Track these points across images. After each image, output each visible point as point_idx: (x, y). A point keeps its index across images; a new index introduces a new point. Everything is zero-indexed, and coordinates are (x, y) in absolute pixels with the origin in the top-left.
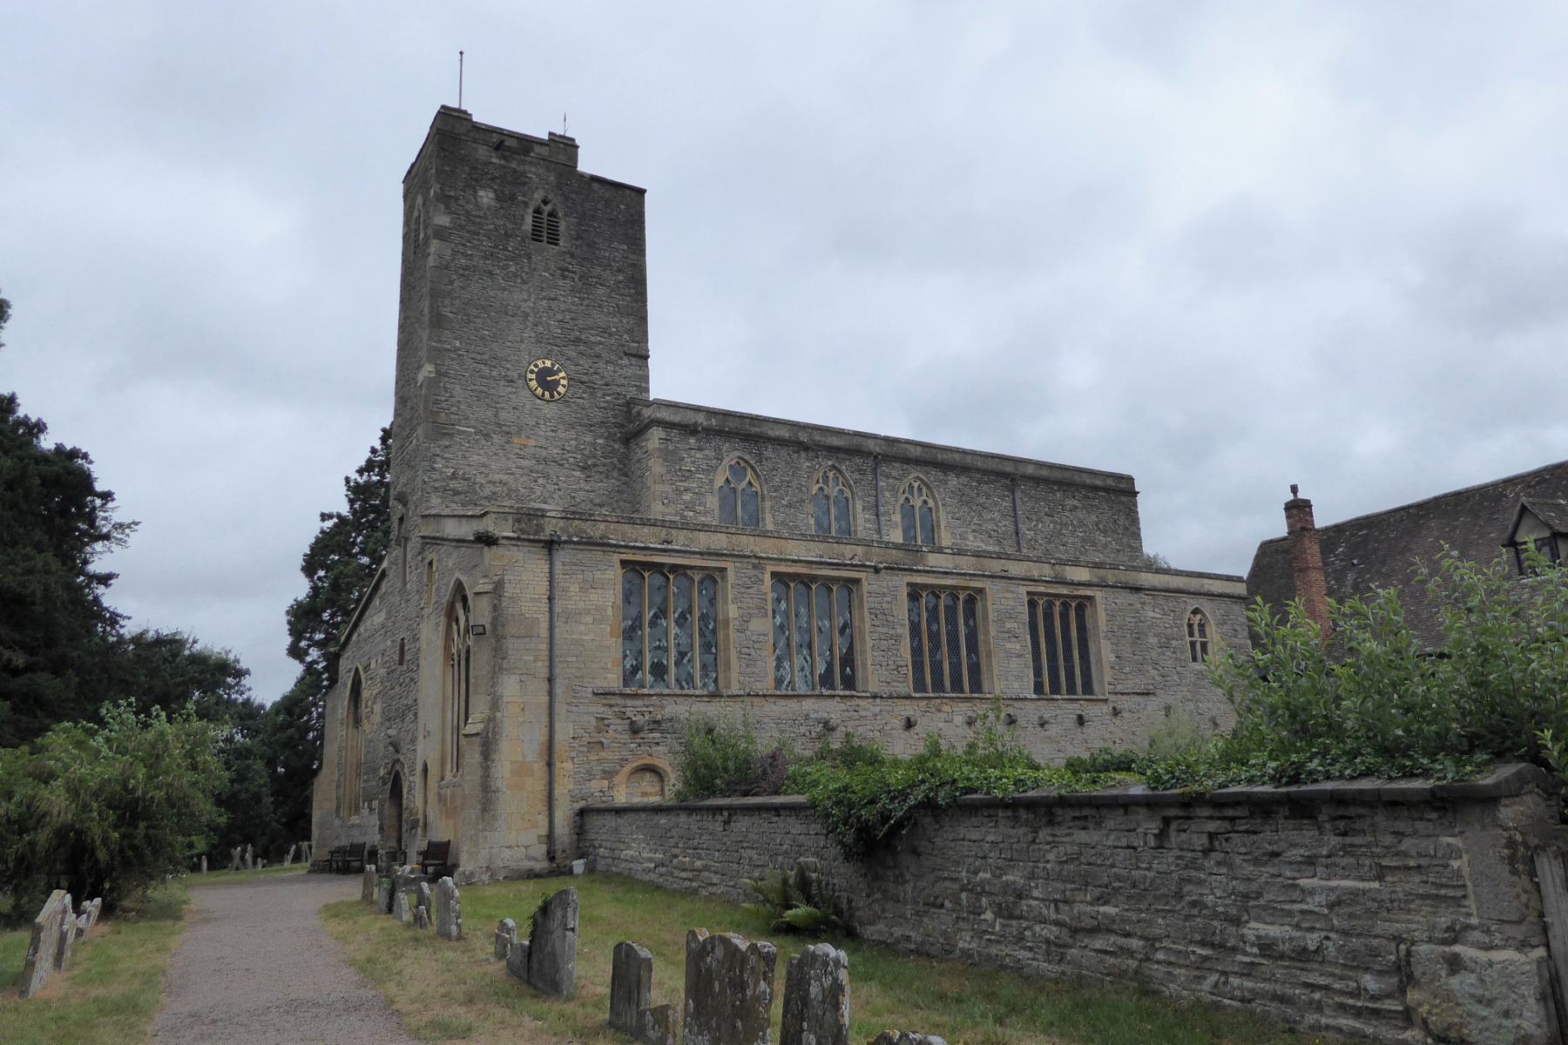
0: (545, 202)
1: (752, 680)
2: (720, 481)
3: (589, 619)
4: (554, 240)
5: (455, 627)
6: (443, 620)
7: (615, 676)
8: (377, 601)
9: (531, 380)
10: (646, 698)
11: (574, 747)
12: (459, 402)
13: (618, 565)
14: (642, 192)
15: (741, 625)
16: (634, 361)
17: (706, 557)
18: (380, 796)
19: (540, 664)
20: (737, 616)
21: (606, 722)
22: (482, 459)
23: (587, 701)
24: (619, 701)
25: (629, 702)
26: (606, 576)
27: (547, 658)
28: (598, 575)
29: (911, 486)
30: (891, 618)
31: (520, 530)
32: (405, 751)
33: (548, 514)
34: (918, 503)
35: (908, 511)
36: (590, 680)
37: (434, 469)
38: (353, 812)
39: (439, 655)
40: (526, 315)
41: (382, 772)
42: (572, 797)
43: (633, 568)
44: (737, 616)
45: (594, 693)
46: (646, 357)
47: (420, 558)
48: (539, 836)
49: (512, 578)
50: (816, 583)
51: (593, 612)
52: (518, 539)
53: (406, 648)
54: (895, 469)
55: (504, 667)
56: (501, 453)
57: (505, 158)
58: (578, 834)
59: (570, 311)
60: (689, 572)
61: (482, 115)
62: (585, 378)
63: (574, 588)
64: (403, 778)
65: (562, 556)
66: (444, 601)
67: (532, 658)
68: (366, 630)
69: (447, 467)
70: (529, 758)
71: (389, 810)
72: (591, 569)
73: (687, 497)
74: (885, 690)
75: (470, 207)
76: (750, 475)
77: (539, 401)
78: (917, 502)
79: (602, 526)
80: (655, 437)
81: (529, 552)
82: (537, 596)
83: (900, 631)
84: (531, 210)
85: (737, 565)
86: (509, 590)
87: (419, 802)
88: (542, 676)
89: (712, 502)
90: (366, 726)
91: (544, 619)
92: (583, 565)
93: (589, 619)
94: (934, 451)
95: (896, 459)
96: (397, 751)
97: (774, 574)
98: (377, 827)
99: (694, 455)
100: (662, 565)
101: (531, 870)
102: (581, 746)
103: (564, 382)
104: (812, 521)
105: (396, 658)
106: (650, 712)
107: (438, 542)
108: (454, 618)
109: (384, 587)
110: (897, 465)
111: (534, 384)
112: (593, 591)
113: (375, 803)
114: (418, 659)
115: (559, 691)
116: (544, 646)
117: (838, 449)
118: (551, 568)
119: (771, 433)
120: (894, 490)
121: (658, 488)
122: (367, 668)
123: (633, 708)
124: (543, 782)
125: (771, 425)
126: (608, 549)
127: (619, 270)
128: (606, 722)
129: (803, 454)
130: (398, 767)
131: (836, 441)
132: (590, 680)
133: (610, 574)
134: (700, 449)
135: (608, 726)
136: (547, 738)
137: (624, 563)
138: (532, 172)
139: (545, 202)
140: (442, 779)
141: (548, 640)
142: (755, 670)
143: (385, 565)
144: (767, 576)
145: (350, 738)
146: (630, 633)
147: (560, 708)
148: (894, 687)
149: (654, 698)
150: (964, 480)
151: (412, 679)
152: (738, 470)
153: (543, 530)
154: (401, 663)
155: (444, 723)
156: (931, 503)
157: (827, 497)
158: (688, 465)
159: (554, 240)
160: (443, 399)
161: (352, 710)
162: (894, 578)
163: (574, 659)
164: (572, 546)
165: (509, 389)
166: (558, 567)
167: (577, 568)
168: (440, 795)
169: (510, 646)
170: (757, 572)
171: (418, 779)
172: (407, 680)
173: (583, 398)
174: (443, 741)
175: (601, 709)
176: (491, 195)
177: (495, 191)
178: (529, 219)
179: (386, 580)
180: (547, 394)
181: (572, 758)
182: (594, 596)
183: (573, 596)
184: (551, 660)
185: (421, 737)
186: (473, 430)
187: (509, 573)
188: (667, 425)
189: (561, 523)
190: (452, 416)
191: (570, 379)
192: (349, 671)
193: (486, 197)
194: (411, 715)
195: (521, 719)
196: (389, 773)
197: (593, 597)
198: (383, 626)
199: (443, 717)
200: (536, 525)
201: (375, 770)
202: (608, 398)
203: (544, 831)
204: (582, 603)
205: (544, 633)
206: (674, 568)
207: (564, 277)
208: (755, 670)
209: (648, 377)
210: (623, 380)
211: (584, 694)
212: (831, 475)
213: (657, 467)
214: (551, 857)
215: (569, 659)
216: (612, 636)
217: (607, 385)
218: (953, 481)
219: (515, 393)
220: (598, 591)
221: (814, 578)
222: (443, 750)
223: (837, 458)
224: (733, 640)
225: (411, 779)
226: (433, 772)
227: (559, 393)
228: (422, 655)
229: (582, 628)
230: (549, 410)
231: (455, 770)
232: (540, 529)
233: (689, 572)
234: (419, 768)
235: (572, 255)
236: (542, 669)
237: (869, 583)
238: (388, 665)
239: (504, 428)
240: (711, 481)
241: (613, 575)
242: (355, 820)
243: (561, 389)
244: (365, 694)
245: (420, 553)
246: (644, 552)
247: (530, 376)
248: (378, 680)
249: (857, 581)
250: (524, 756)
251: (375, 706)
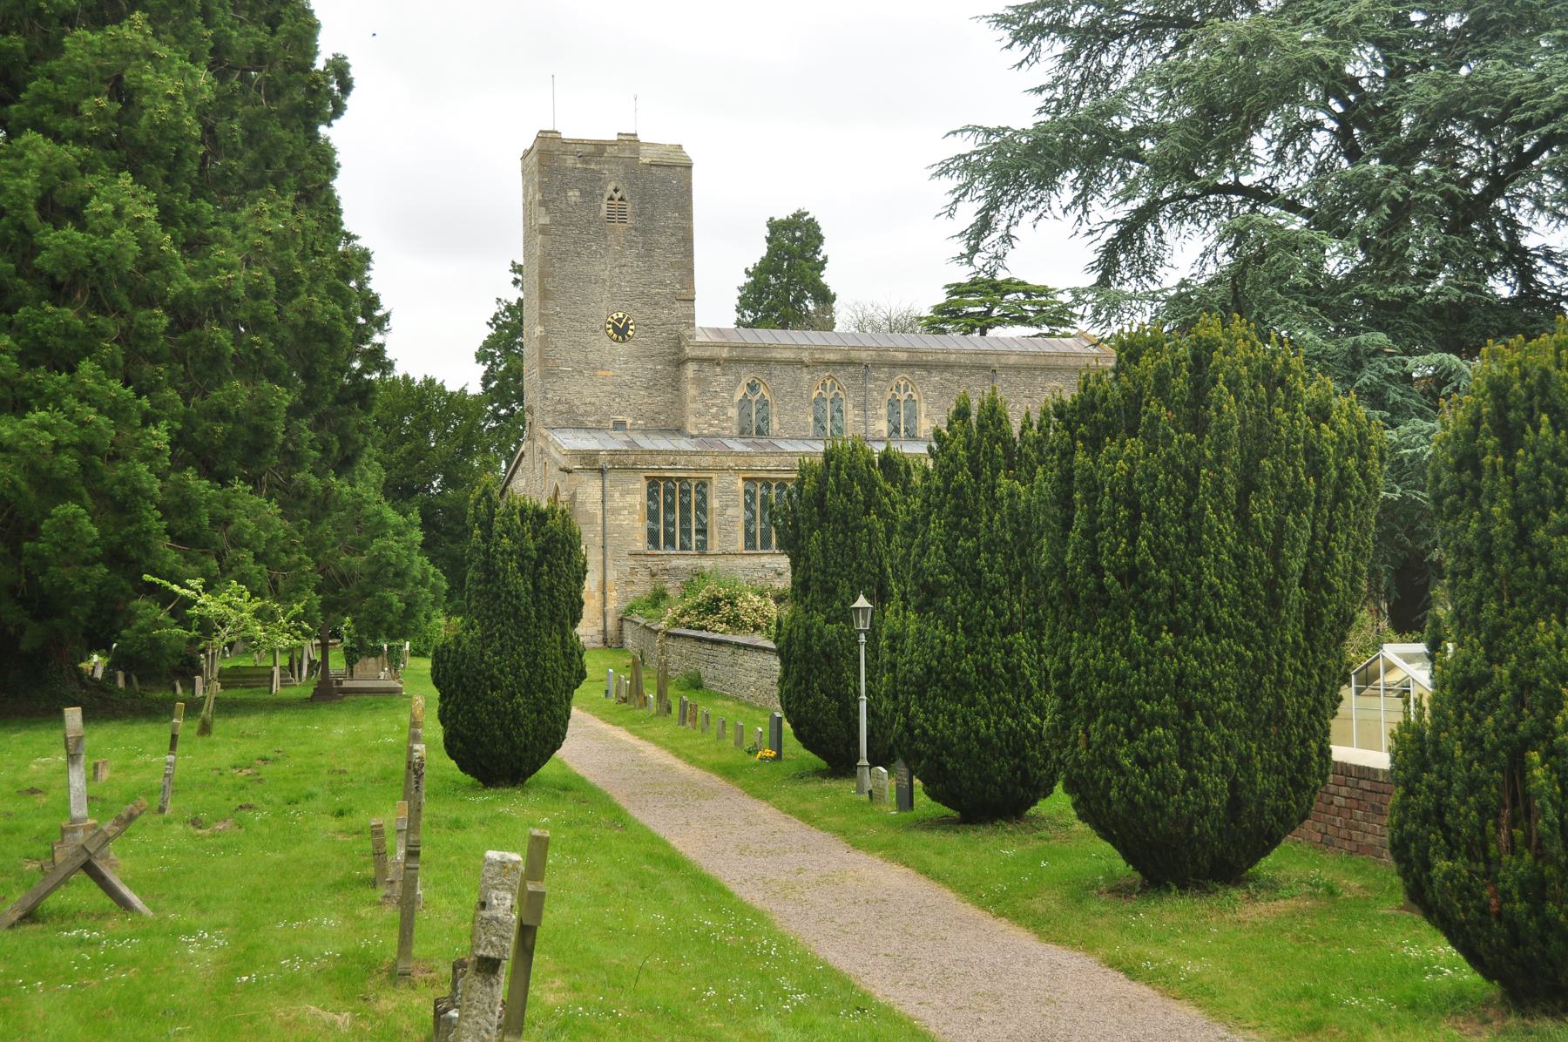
0: (616, 191)
2: (738, 396)
4: (623, 220)
8: (519, 471)
14: (689, 167)
16: (683, 304)
22: (577, 389)
25: (650, 559)
29: (898, 387)
34: (903, 397)
35: (893, 403)
40: (604, 281)
43: (653, 483)
54: (883, 373)
56: (590, 383)
57: (587, 162)
59: (636, 273)
61: (567, 134)
65: (610, 476)
73: (714, 410)
75: (563, 206)
76: (762, 390)
78: (903, 397)
79: (633, 457)
80: (690, 370)
84: (605, 200)
86: (580, 498)
89: (733, 412)
93: (626, 512)
95: (884, 364)
99: (720, 379)
104: (811, 419)
109: (523, 463)
111: (611, 331)
117: (834, 363)
119: (779, 356)
120: (882, 392)
121: (691, 405)
123: (650, 562)
127: (672, 235)
129: (805, 370)
133: (638, 485)
134: (724, 375)
138: (606, 170)
139: (616, 191)
143: (523, 448)
146: (652, 515)
147: (609, 563)
150: (947, 375)
152: (752, 387)
156: (915, 397)
157: (825, 400)
158: (715, 387)
159: (623, 220)
166: (607, 483)
176: (577, 193)
177: (580, 190)
178: (604, 207)
182: (629, 499)
183: (616, 500)
188: (700, 360)
193: (574, 195)
203: (601, 628)
205: (600, 521)
206: (679, 479)
207: (631, 247)
212: (829, 383)
213: (692, 391)
214: (605, 641)
218: (936, 378)
224: (713, 521)
230: (621, 348)
232: (596, 461)
235: (636, 230)
240: (732, 397)
241: (641, 485)
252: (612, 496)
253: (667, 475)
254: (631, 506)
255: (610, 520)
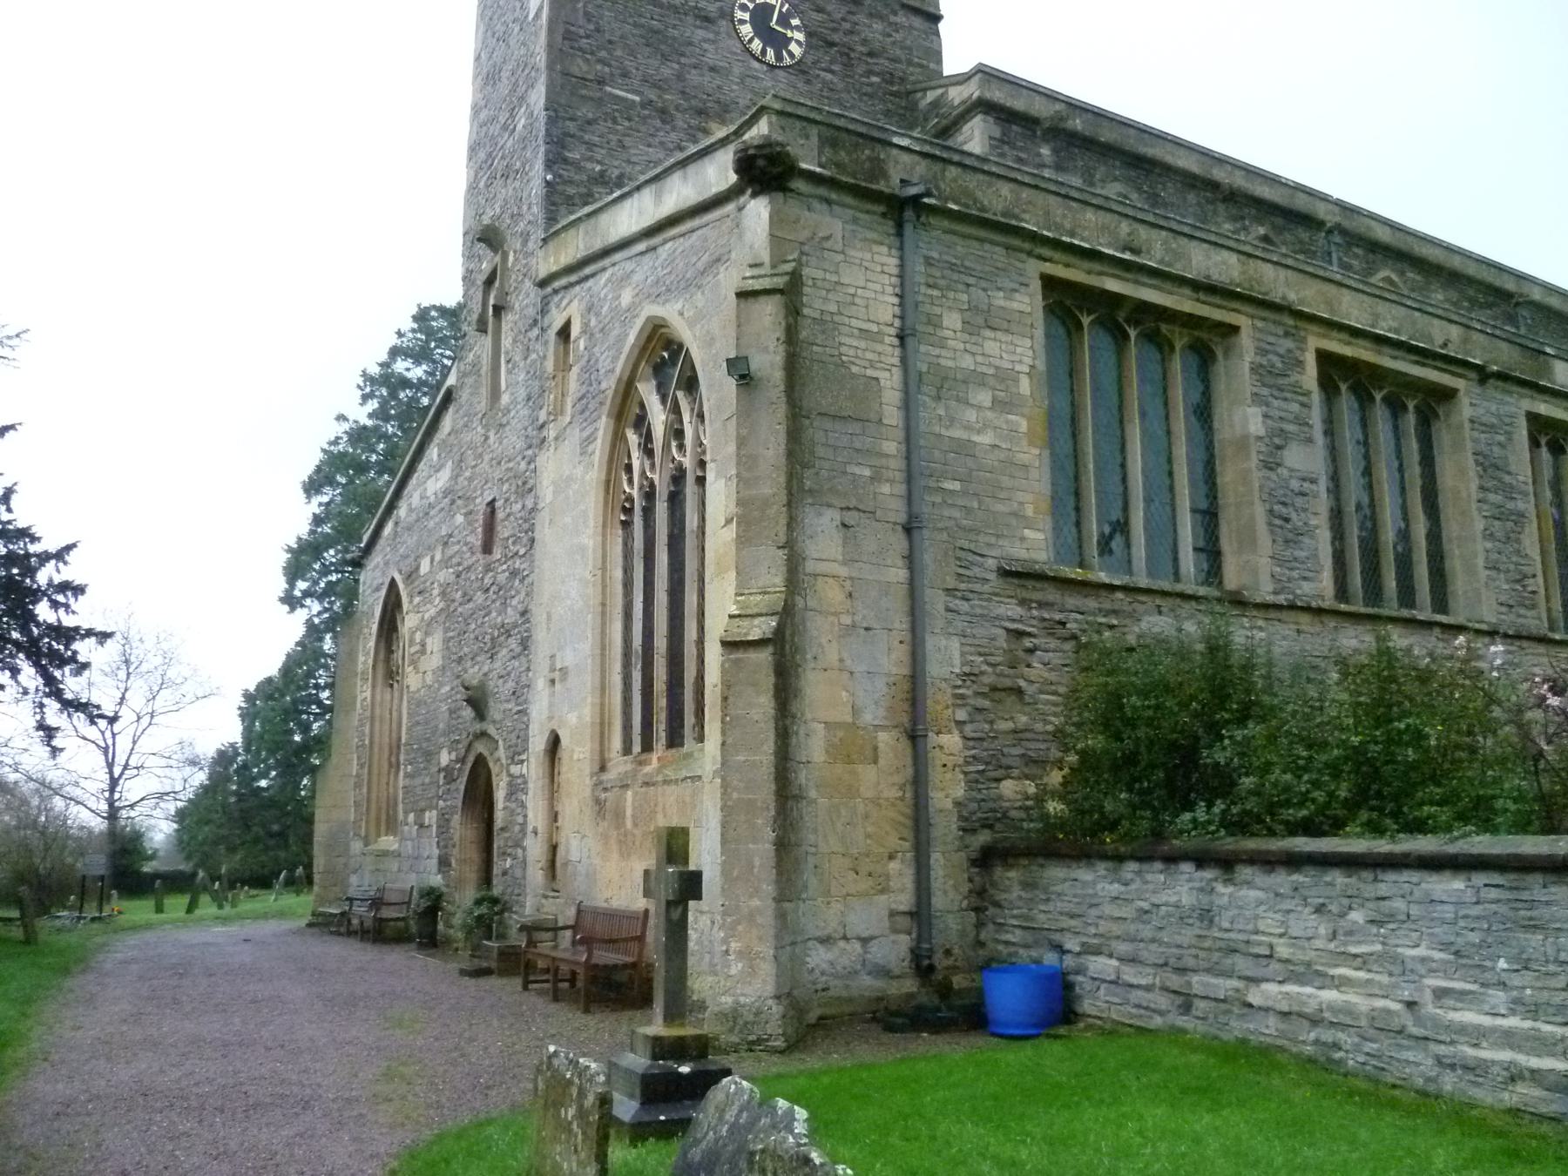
1: (1295, 574)
3: (984, 397)
5: (633, 438)
6: (604, 425)
7: (1040, 536)
8: (433, 453)
9: (742, 22)
10: (1104, 593)
11: (962, 697)
12: (610, 42)
13: (1036, 285)
15: (1271, 454)
17: (1202, 296)
18: (441, 803)
19: (886, 489)
20: (1262, 432)
21: (1028, 643)
23: (986, 588)
24: (1051, 594)
25: (1072, 601)
26: (1015, 305)
27: (900, 476)
28: (999, 299)
30: (1507, 479)
31: (838, 165)
32: (497, 717)
33: (896, 140)
36: (993, 540)
37: (565, 161)
38: (383, 828)
39: (592, 503)
41: (445, 758)
42: (961, 818)
44: (1262, 432)
45: (1005, 574)
46: (936, 18)
47: (536, 331)
48: (893, 914)
49: (819, 274)
50: (1381, 388)
51: (992, 382)
52: (831, 183)
53: (500, 515)
55: (808, 484)
58: (977, 910)
60: (1164, 328)
62: (836, 37)
63: (952, 320)
64: (494, 769)
66: (609, 384)
67: (867, 472)
68: (411, 510)
69: (590, 159)
70: (868, 718)
71: (462, 829)
72: (984, 284)
74: (1509, 621)
77: (756, 65)
79: (1005, 189)
81: (855, 221)
82: (874, 328)
83: (1521, 505)
85: (1260, 324)
86: (814, 303)
87: (536, 815)
88: (892, 517)
90: (412, 680)
91: (890, 382)
92: (968, 271)
93: (984, 397)
94: (1410, 239)
96: (481, 714)
97: (1324, 357)
98: (435, 861)
100: (1116, 299)
101: (879, 999)
102: (977, 694)
103: (800, 36)
105: (476, 540)
106: (1111, 627)
107: (588, 270)
108: (632, 418)
110: (1359, 251)
111: (746, 30)
112: (988, 333)
113: (431, 817)
114: (532, 529)
115: (929, 558)
116: (891, 447)
118: (902, 266)
119: (1169, 159)
122: (410, 576)
124: (898, 779)
125: (1169, 146)
126: (1016, 242)
128: (1028, 643)
129: (1221, 207)
130: (480, 747)
131: (1264, 192)
132: (993, 540)
134: (1058, 168)
135: (1031, 651)
136: (906, 671)
137: (1049, 283)
140: (603, 768)
141: (901, 435)
142: (1298, 553)
144: (1310, 360)
145: (378, 697)
148: (1519, 616)
149: (1119, 595)
151: (514, 573)
153: (884, 175)
154: (487, 548)
155: (603, 648)
160: (582, 32)
161: (382, 656)
162: (1508, 399)
163: (957, 486)
164: (946, 224)
165: (701, 33)
167: (955, 276)
168: (597, 801)
169: (819, 436)
170: (1289, 344)
171: (533, 768)
172: (502, 578)
173: (832, 72)
174: (603, 688)
175: (1015, 610)
179: (451, 410)
180: (770, 53)
181: (960, 724)
182: (993, 345)
184: (909, 480)
185: (541, 684)
186: (637, 99)
187: (813, 261)
189: (921, 168)
190: (599, 67)
191: (809, 35)
192: (378, 589)
194: (513, 643)
195: (846, 620)
196: (463, 760)
197: (991, 347)
198: (447, 492)
199: (603, 633)
200: (869, 159)
201: (430, 755)
202: (875, 79)
203: (904, 900)
204: (968, 357)
205: (892, 415)
208: (1298, 553)
209: (939, 53)
210: (898, 52)
211: (976, 571)
215: (948, 485)
216: (1031, 444)
217: (871, 54)
219: (714, 42)
220: (999, 335)
221: (1377, 374)
222: (602, 705)
223: (1273, 224)
225: (515, 770)
226: (578, 755)
227: (791, 55)
228: (542, 520)
229: (971, 415)
231: (637, 748)
232: (878, 170)
233: (1164, 328)
234: (538, 744)
236: (890, 493)
237: (1472, 403)
238: (455, 561)
239: (693, 102)
241: (1028, 302)
242: (388, 842)
243: (793, 47)
244: (409, 622)
245: (535, 322)
246: (1087, 265)
247: (739, 14)
248: (436, 592)
249: (1448, 395)
250: (855, 711)
251: (429, 641)
252: (935, 322)
253: (1113, 285)
254: (1005, 377)
255: (931, 412)
